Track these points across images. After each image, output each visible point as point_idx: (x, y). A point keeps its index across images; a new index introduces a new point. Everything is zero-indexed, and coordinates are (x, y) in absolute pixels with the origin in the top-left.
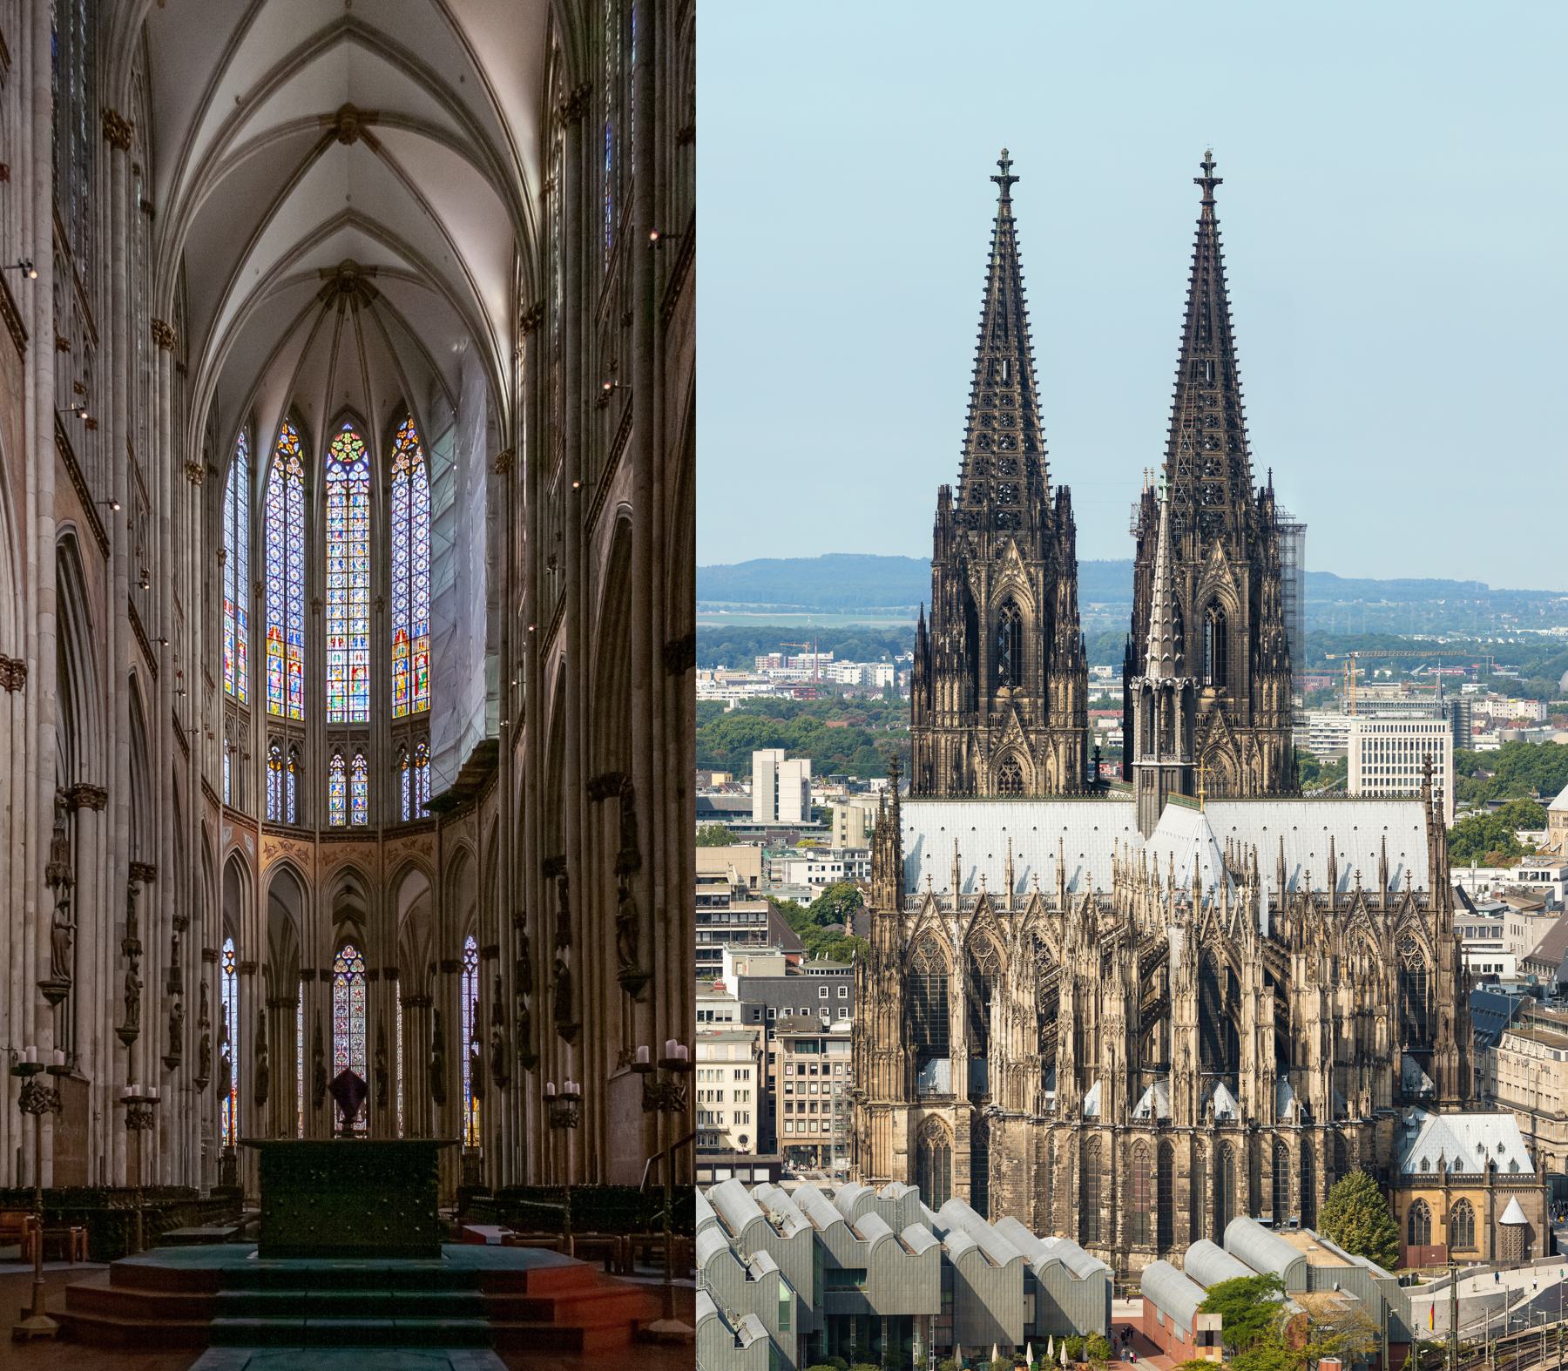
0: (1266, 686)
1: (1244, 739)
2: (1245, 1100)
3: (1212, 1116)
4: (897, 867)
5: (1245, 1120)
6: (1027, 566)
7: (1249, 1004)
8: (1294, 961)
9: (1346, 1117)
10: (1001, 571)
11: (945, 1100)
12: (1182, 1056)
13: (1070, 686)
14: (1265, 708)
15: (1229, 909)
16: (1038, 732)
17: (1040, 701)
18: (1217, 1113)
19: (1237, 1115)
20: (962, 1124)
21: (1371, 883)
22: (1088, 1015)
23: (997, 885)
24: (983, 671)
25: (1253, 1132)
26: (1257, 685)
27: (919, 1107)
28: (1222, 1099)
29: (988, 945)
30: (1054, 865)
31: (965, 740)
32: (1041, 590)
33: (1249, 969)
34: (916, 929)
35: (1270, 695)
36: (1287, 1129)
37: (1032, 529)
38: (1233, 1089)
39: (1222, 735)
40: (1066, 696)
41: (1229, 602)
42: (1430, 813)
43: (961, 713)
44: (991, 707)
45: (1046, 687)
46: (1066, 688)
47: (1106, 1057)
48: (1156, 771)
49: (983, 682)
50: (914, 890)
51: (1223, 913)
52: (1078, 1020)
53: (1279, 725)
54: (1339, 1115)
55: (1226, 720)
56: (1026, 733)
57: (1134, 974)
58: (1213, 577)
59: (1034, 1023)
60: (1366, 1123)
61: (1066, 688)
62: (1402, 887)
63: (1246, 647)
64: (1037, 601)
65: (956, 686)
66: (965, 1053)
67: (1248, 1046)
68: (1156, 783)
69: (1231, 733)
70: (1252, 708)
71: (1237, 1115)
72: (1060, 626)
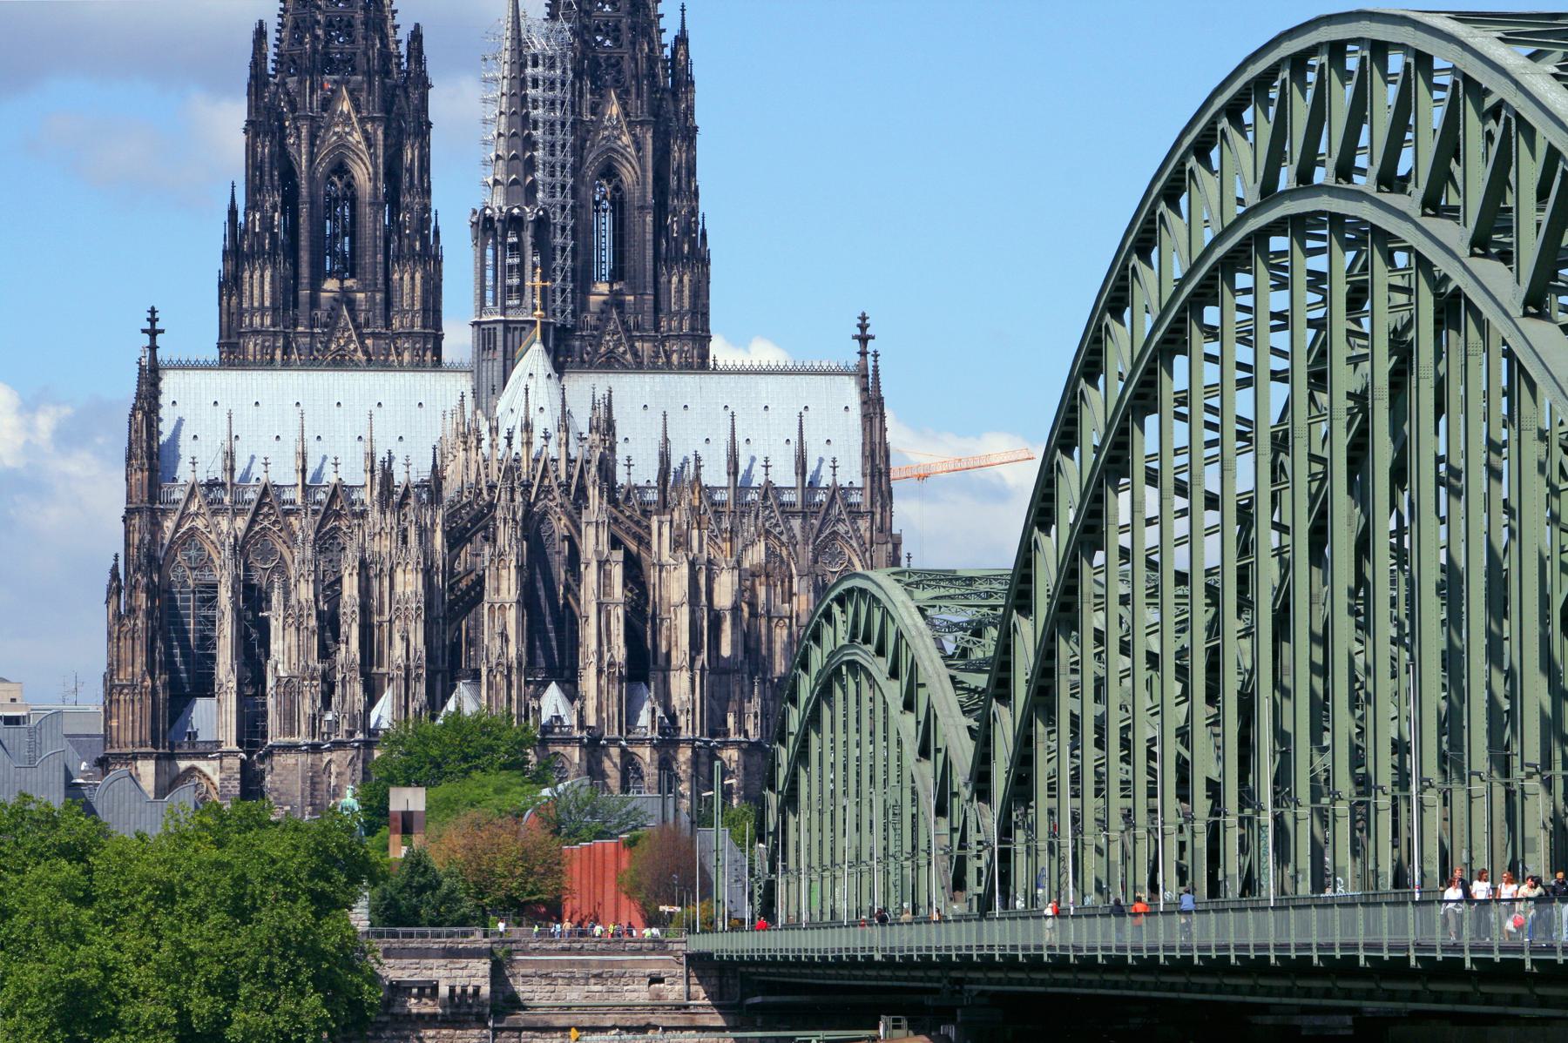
0: (675, 279)
1: (645, 348)
2: (583, 699)
3: (537, 721)
4: (150, 447)
5: (582, 724)
6: (362, 121)
7: (591, 576)
8: (655, 526)
9: (726, 733)
10: (328, 129)
11: (211, 750)
12: (498, 642)
13: (418, 276)
14: (674, 308)
15: (570, 461)
16: (374, 335)
17: (379, 296)
18: (545, 719)
19: (571, 719)
20: (229, 778)
21: (784, 476)
22: (381, 603)
23: (284, 473)
24: (304, 256)
25: (594, 746)
26: (664, 279)
27: (172, 757)
28: (552, 701)
29: (273, 551)
30: (362, 449)
31: (280, 343)
32: (380, 152)
33: (591, 531)
34: (176, 531)
35: (680, 291)
36: (641, 742)
37: (369, 74)
38: (572, 693)
39: (618, 343)
40: (413, 285)
41: (628, 175)
42: (865, 389)
43: (274, 309)
44: (314, 302)
45: (387, 279)
46: (413, 278)
47: (399, 649)
48: (500, 327)
49: (305, 270)
50: (175, 480)
51: (562, 465)
52: (365, 609)
53: (692, 329)
54: (716, 727)
55: (623, 323)
56: (361, 337)
57: (439, 539)
58: (607, 138)
59: (313, 623)
60: (755, 746)
61: (413, 278)
62: (826, 480)
63: (649, 228)
64: (375, 166)
65: (268, 274)
66: (233, 684)
67: (589, 634)
68: (500, 343)
69: (631, 339)
70: (657, 309)
71: (571, 719)
72: (406, 199)
